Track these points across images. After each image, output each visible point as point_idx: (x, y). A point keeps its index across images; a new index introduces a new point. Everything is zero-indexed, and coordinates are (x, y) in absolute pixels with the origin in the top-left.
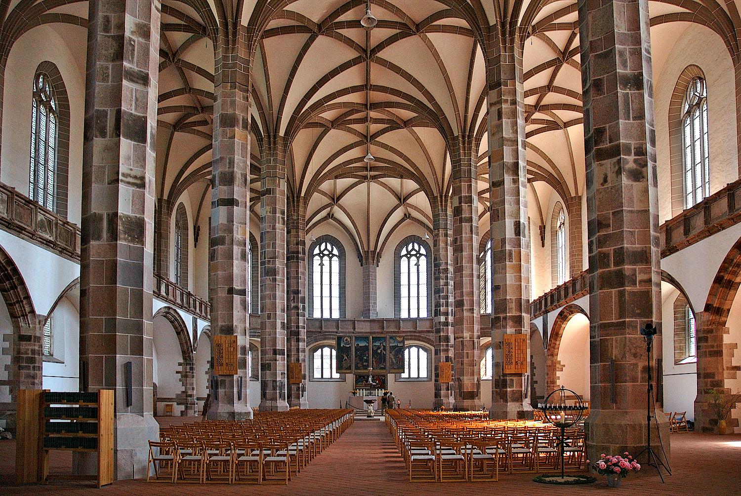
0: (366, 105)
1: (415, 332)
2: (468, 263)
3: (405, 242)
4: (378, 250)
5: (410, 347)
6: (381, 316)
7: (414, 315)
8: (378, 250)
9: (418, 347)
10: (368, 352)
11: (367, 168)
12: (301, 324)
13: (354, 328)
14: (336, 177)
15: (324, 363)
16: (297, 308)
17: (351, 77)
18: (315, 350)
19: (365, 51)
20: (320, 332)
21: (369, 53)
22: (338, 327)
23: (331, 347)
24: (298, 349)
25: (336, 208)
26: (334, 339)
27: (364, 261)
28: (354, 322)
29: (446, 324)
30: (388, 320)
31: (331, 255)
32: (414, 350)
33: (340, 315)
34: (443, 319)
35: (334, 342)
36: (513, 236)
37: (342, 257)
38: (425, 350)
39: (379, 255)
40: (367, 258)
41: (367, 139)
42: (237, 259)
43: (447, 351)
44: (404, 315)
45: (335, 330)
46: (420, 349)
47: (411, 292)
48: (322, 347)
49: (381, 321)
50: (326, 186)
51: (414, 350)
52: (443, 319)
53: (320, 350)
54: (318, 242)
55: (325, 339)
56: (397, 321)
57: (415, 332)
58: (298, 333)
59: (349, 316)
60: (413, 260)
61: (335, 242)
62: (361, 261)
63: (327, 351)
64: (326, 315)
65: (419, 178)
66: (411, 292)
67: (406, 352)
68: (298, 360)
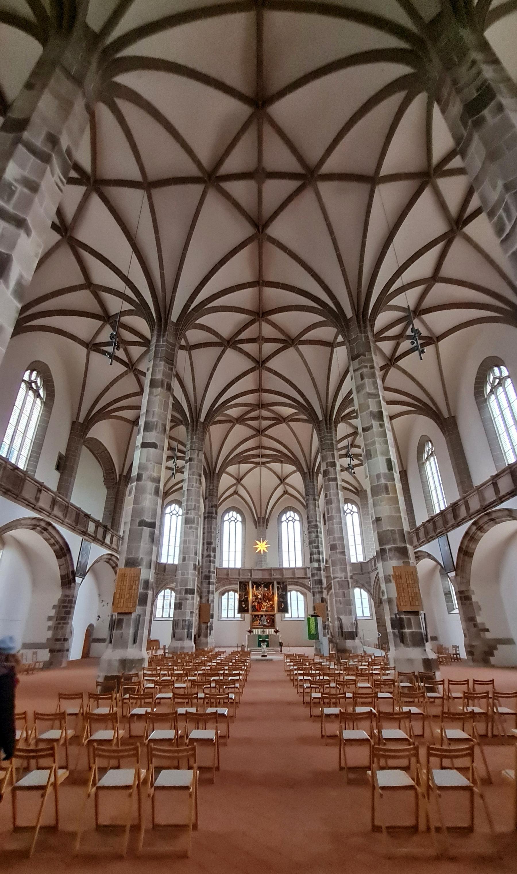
0: (258, 405)
1: (293, 578)
2: (337, 513)
3: (284, 511)
4: (267, 517)
5: (290, 591)
6: (269, 566)
7: (292, 565)
8: (267, 517)
9: (297, 591)
10: (263, 590)
11: (259, 455)
12: (212, 570)
13: (251, 576)
14: (240, 463)
15: (228, 605)
16: (209, 556)
17: (248, 383)
18: (223, 594)
19: (257, 362)
20: (226, 578)
21: (261, 363)
22: (239, 575)
23: (235, 591)
24: (209, 592)
25: (240, 487)
26: (236, 584)
27: (258, 524)
28: (250, 570)
29: (319, 569)
30: (275, 570)
31: (236, 521)
32: (294, 593)
33: (242, 565)
34: (316, 565)
35: (237, 587)
36: (387, 471)
37: (244, 522)
38: (302, 593)
39: (268, 520)
40: (259, 523)
41: (260, 432)
42: (151, 494)
43: (321, 592)
44: (286, 565)
45: (238, 577)
46: (299, 593)
47: (290, 546)
48: (228, 591)
49: (270, 570)
50: (231, 469)
51: (294, 593)
52: (316, 565)
53: (227, 593)
54: (227, 511)
55: (231, 584)
56: (281, 570)
57: (293, 578)
58: (208, 577)
59: (248, 567)
60: (291, 523)
61: (239, 511)
62: (256, 525)
63: (231, 593)
64: (232, 566)
65: (294, 461)
66: (290, 546)
67: (289, 594)
68: (208, 601)
